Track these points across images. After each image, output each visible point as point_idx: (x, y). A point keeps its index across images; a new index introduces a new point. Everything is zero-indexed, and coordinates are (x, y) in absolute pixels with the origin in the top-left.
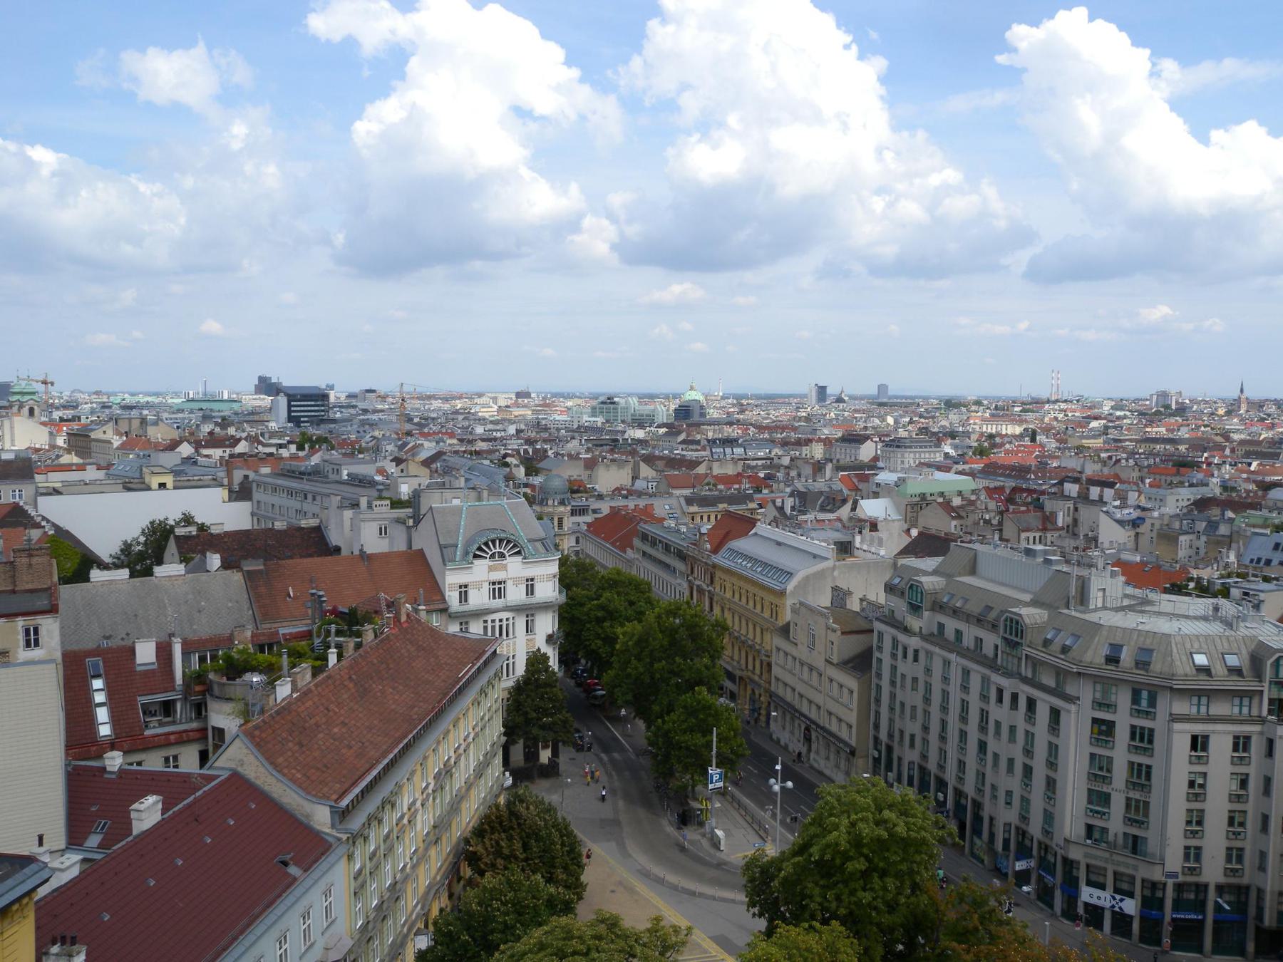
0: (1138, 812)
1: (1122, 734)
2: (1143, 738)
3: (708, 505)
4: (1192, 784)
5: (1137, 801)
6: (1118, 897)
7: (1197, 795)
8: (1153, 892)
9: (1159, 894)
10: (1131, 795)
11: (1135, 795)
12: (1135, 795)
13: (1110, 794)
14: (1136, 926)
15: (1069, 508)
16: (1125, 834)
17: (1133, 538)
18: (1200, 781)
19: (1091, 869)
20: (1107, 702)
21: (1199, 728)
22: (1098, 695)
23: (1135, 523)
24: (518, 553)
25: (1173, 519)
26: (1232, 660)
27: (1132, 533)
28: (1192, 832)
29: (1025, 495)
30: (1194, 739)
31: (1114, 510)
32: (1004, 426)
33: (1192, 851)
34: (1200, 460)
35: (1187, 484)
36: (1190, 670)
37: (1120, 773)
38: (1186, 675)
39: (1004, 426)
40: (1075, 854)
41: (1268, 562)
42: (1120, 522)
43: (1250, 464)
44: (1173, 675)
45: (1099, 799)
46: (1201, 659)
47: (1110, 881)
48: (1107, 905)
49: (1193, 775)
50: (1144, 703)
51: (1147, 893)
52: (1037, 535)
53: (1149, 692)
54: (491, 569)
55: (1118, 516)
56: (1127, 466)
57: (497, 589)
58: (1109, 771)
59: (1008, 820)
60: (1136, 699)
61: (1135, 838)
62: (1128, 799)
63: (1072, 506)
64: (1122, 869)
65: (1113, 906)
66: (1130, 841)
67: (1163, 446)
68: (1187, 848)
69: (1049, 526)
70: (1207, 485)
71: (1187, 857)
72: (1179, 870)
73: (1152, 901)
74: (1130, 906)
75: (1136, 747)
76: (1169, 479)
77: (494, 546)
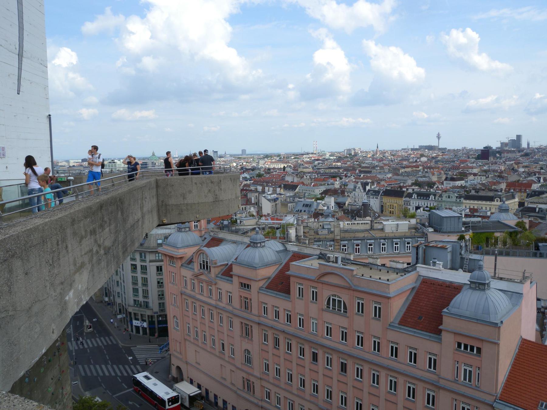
0: (146, 294)
1: (139, 268)
2: (144, 269)
4: (158, 282)
5: (145, 290)
6: (142, 322)
7: (160, 286)
8: (152, 319)
9: (154, 319)
10: (143, 288)
11: (144, 288)
12: (144, 288)
13: (138, 289)
14: (148, 331)
15: (256, 196)
16: (144, 301)
17: (274, 206)
18: (162, 281)
19: (143, 316)
20: (134, 258)
21: (158, 264)
22: (132, 256)
23: (275, 200)
25: (287, 198)
27: (274, 204)
28: (160, 298)
29: (245, 192)
30: (158, 267)
31: (267, 196)
32: (280, 165)
33: (162, 304)
34: (343, 175)
35: (326, 184)
36: (155, 245)
37: (140, 282)
38: (153, 247)
39: (280, 165)
40: (130, 310)
41: (301, 211)
42: (269, 200)
43: (360, 175)
44: (149, 247)
45: (136, 291)
47: (140, 317)
48: (140, 325)
49: (158, 280)
50: (143, 257)
51: (150, 319)
52: (244, 207)
53: (144, 253)
55: (269, 197)
56: (306, 179)
58: (137, 281)
59: (119, 302)
60: (141, 257)
61: (146, 302)
62: (143, 290)
63: (257, 195)
64: (142, 313)
65: (141, 325)
66: (145, 304)
67: (329, 170)
68: (160, 304)
69: (248, 203)
70: (334, 184)
71: (160, 307)
72: (158, 311)
73: (151, 323)
75: (143, 272)
76: (321, 182)
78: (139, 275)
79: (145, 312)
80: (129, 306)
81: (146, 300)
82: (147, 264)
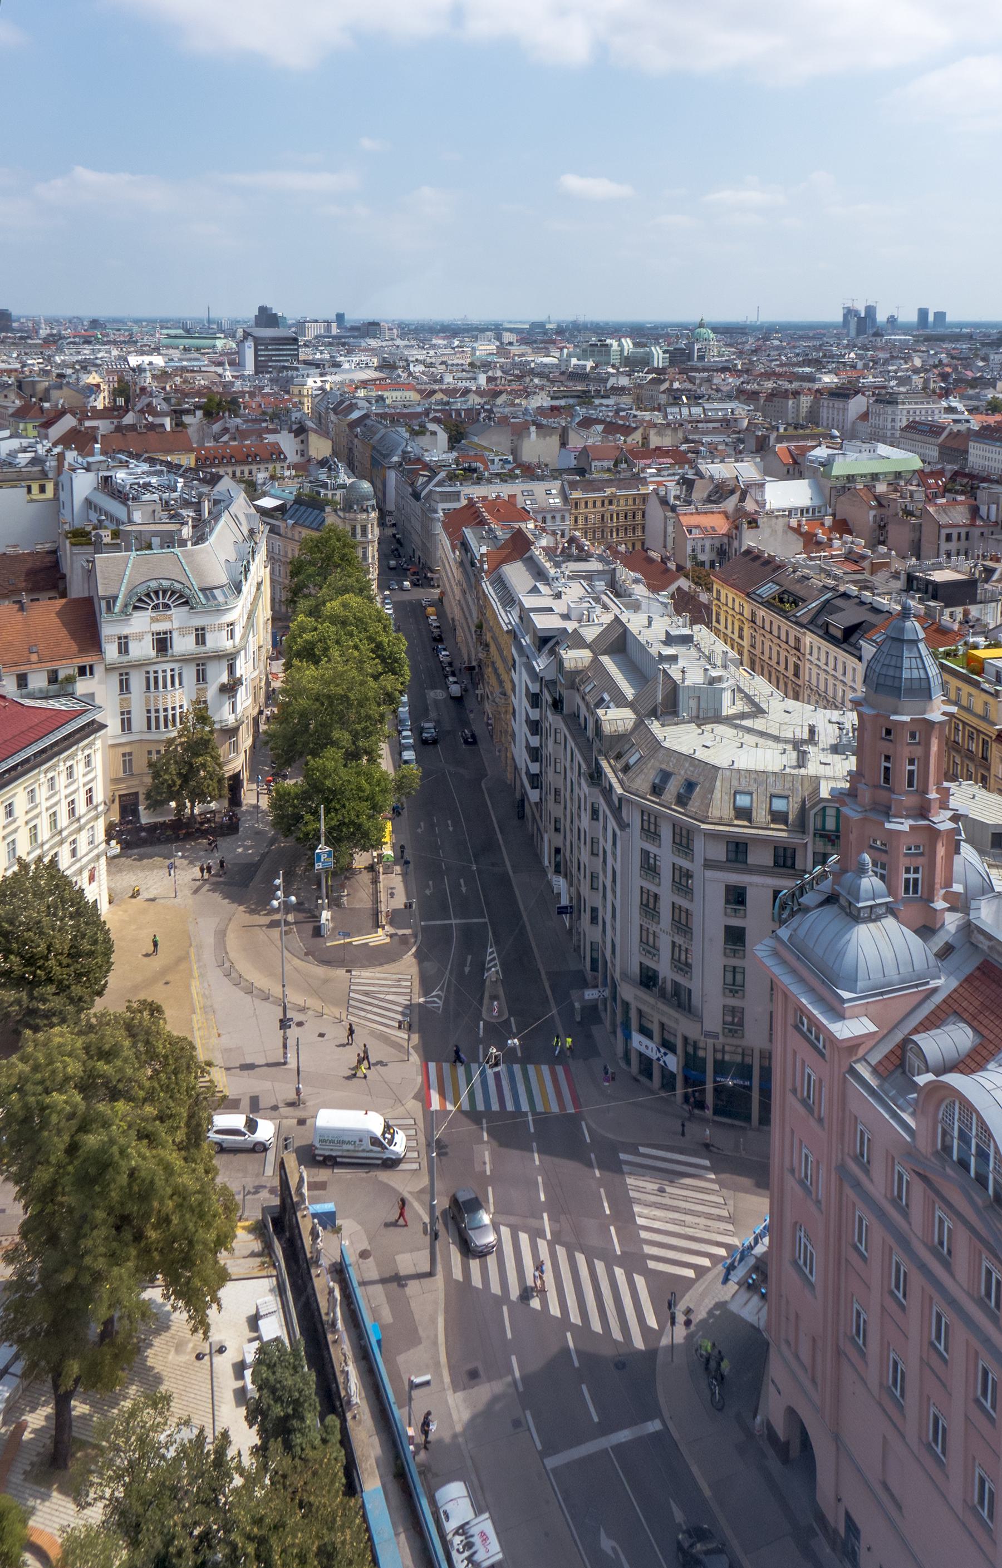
3: (594, 491)
6: (662, 1050)
11: (679, 940)
24: (186, 603)
26: (779, 805)
40: (628, 992)
46: (743, 801)
51: (690, 1050)
54: (154, 620)
57: (162, 643)
62: (674, 943)
64: (665, 1020)
65: (658, 1059)
73: (693, 1063)
74: (673, 1063)
77: (158, 598)
78: (665, 889)
79: (677, 1021)
80: (624, 975)
81: (679, 979)
82: (695, 866)
